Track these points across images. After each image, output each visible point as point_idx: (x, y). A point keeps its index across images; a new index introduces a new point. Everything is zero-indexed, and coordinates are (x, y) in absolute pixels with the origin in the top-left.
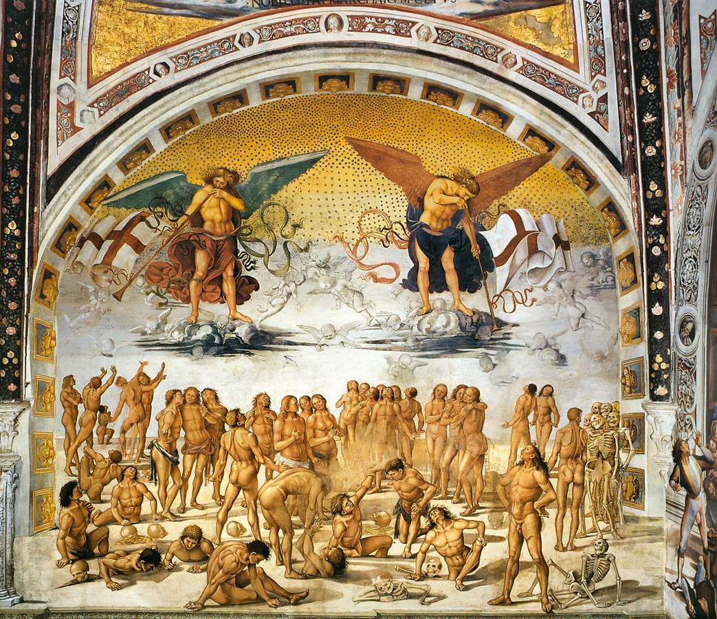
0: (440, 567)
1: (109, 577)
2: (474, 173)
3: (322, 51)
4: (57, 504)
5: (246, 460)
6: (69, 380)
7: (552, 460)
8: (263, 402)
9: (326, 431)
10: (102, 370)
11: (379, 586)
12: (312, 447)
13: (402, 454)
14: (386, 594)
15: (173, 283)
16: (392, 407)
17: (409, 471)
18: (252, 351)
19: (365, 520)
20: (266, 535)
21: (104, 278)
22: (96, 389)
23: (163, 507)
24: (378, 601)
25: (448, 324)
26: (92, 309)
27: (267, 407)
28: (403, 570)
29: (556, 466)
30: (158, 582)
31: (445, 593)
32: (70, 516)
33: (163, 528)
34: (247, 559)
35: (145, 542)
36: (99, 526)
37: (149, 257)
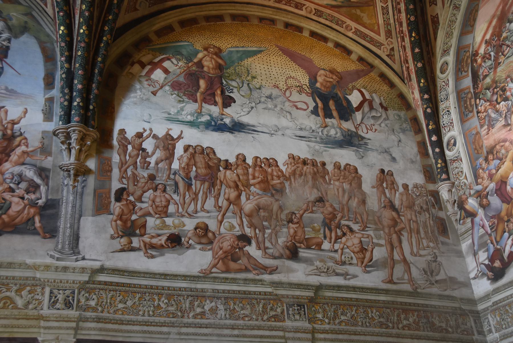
0: (352, 258)
1: (146, 249)
2: (339, 71)
3: (261, 7)
4: (113, 199)
5: (234, 188)
6: (122, 132)
7: (400, 207)
8: (242, 159)
9: (279, 177)
10: (144, 129)
11: (319, 267)
12: (272, 185)
13: (322, 194)
14: (324, 272)
15: (187, 91)
16: (313, 169)
17: (327, 204)
18: (234, 132)
19: (306, 227)
20: (248, 231)
21: (146, 83)
22: (140, 138)
23: (183, 209)
24: (320, 275)
25: (337, 133)
26: (138, 97)
27: (244, 160)
28: (332, 258)
29: (402, 211)
30: (180, 255)
31: (356, 273)
32: (120, 208)
33: (183, 222)
34: (238, 245)
35: (170, 230)
36: (140, 217)
37: (171, 77)
